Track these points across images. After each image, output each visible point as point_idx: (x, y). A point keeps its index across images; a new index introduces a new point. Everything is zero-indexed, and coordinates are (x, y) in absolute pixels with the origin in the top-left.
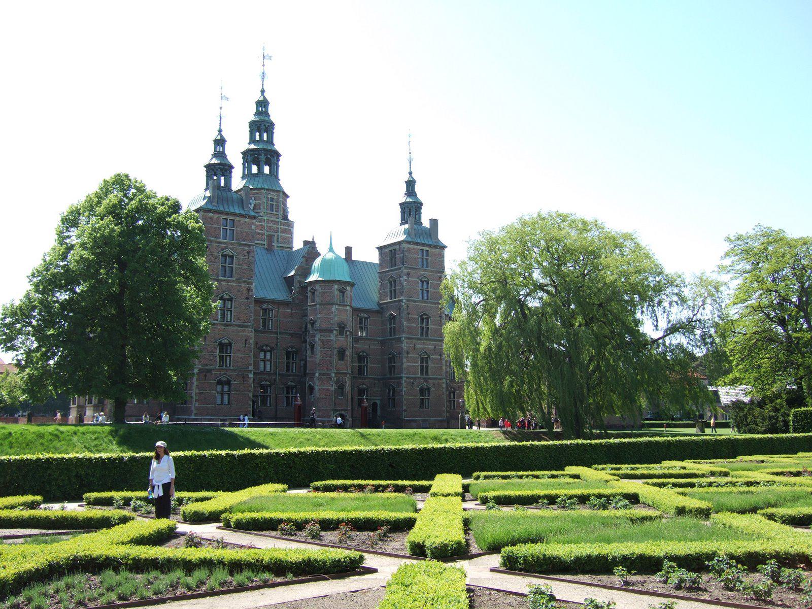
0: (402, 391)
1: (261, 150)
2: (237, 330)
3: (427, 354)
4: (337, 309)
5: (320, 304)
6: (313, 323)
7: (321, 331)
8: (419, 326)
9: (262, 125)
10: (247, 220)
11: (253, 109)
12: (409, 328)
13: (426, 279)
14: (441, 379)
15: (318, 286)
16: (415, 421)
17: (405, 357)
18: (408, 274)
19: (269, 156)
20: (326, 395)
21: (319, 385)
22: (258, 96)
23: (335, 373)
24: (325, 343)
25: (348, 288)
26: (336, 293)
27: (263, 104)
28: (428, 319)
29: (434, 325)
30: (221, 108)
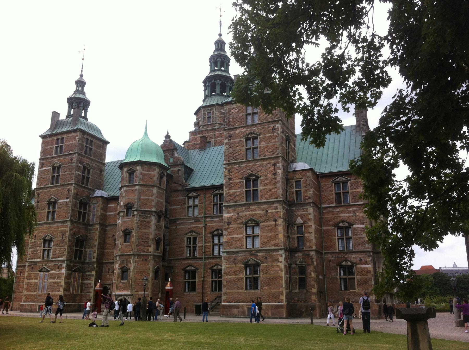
2: (57, 226)
3: (254, 220)
4: (125, 191)
8: (245, 190)
10: (72, 134)
12: (230, 195)
13: (254, 135)
14: (277, 250)
16: (237, 307)
17: (226, 229)
18: (230, 137)
19: (213, 81)
23: (120, 256)
25: (138, 168)
28: (256, 180)
29: (267, 185)
30: (83, 60)
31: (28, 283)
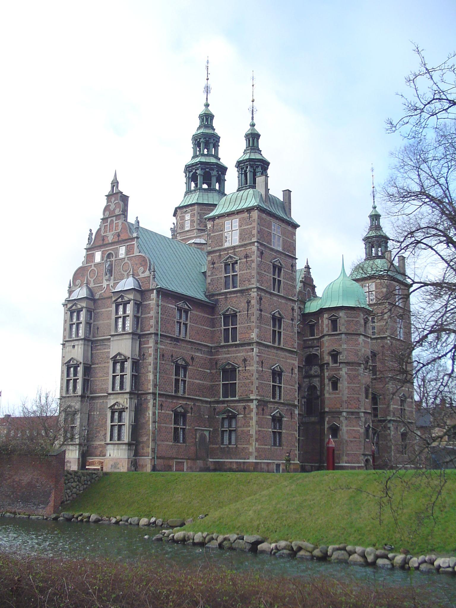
0: (390, 434)
1: (214, 165)
4: (363, 340)
5: (346, 334)
6: (335, 355)
7: (348, 364)
9: (207, 140)
11: (197, 122)
15: (341, 314)
20: (354, 438)
21: (347, 426)
22: (201, 109)
23: (364, 412)
24: (352, 378)
26: (362, 322)
27: (207, 119)
31: (259, 431)
